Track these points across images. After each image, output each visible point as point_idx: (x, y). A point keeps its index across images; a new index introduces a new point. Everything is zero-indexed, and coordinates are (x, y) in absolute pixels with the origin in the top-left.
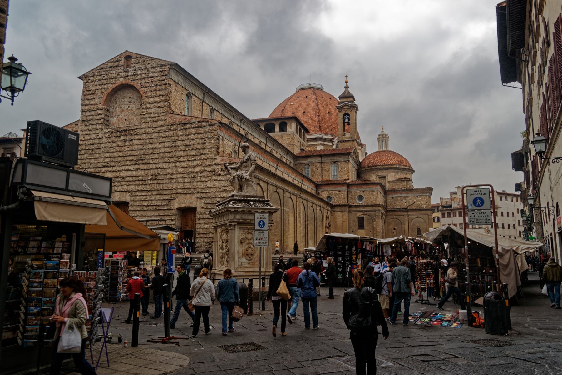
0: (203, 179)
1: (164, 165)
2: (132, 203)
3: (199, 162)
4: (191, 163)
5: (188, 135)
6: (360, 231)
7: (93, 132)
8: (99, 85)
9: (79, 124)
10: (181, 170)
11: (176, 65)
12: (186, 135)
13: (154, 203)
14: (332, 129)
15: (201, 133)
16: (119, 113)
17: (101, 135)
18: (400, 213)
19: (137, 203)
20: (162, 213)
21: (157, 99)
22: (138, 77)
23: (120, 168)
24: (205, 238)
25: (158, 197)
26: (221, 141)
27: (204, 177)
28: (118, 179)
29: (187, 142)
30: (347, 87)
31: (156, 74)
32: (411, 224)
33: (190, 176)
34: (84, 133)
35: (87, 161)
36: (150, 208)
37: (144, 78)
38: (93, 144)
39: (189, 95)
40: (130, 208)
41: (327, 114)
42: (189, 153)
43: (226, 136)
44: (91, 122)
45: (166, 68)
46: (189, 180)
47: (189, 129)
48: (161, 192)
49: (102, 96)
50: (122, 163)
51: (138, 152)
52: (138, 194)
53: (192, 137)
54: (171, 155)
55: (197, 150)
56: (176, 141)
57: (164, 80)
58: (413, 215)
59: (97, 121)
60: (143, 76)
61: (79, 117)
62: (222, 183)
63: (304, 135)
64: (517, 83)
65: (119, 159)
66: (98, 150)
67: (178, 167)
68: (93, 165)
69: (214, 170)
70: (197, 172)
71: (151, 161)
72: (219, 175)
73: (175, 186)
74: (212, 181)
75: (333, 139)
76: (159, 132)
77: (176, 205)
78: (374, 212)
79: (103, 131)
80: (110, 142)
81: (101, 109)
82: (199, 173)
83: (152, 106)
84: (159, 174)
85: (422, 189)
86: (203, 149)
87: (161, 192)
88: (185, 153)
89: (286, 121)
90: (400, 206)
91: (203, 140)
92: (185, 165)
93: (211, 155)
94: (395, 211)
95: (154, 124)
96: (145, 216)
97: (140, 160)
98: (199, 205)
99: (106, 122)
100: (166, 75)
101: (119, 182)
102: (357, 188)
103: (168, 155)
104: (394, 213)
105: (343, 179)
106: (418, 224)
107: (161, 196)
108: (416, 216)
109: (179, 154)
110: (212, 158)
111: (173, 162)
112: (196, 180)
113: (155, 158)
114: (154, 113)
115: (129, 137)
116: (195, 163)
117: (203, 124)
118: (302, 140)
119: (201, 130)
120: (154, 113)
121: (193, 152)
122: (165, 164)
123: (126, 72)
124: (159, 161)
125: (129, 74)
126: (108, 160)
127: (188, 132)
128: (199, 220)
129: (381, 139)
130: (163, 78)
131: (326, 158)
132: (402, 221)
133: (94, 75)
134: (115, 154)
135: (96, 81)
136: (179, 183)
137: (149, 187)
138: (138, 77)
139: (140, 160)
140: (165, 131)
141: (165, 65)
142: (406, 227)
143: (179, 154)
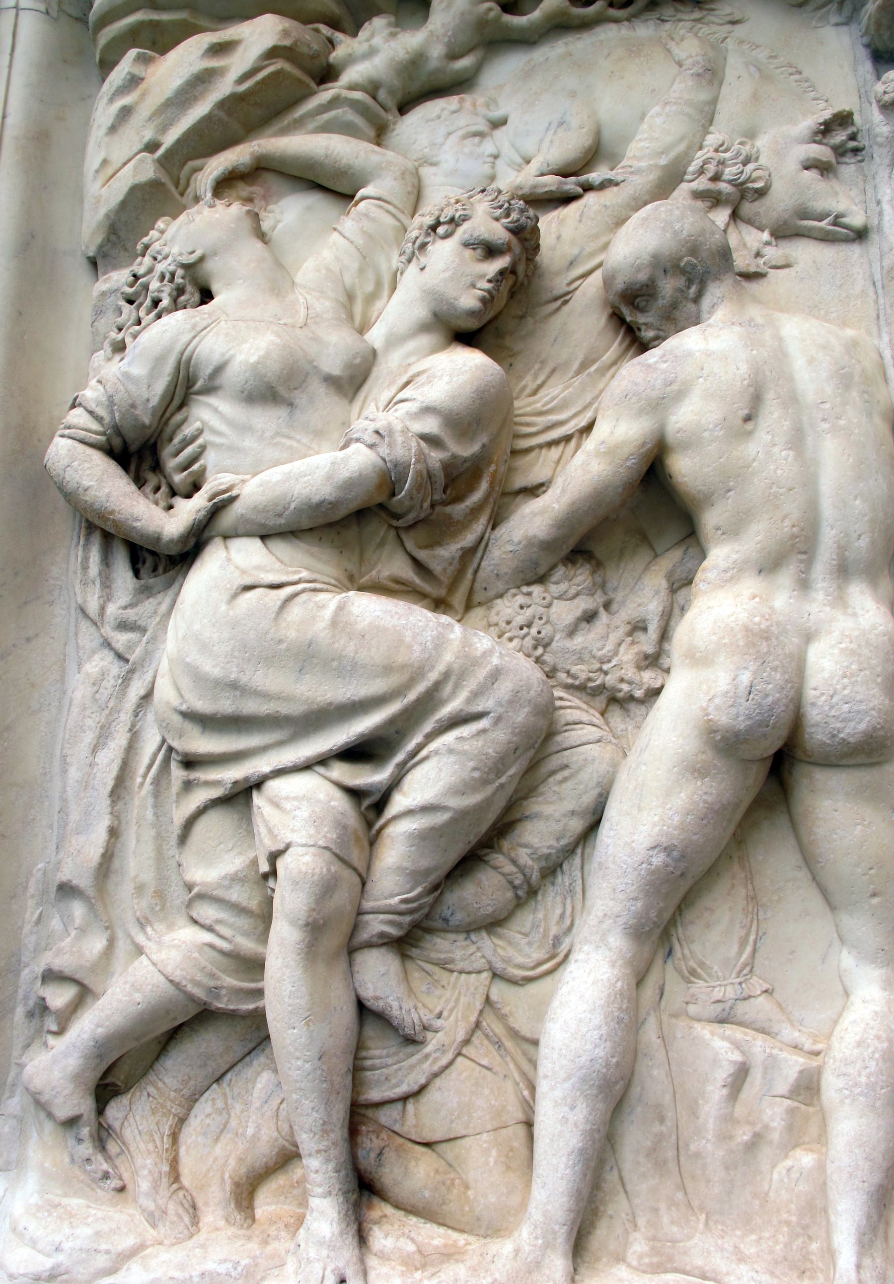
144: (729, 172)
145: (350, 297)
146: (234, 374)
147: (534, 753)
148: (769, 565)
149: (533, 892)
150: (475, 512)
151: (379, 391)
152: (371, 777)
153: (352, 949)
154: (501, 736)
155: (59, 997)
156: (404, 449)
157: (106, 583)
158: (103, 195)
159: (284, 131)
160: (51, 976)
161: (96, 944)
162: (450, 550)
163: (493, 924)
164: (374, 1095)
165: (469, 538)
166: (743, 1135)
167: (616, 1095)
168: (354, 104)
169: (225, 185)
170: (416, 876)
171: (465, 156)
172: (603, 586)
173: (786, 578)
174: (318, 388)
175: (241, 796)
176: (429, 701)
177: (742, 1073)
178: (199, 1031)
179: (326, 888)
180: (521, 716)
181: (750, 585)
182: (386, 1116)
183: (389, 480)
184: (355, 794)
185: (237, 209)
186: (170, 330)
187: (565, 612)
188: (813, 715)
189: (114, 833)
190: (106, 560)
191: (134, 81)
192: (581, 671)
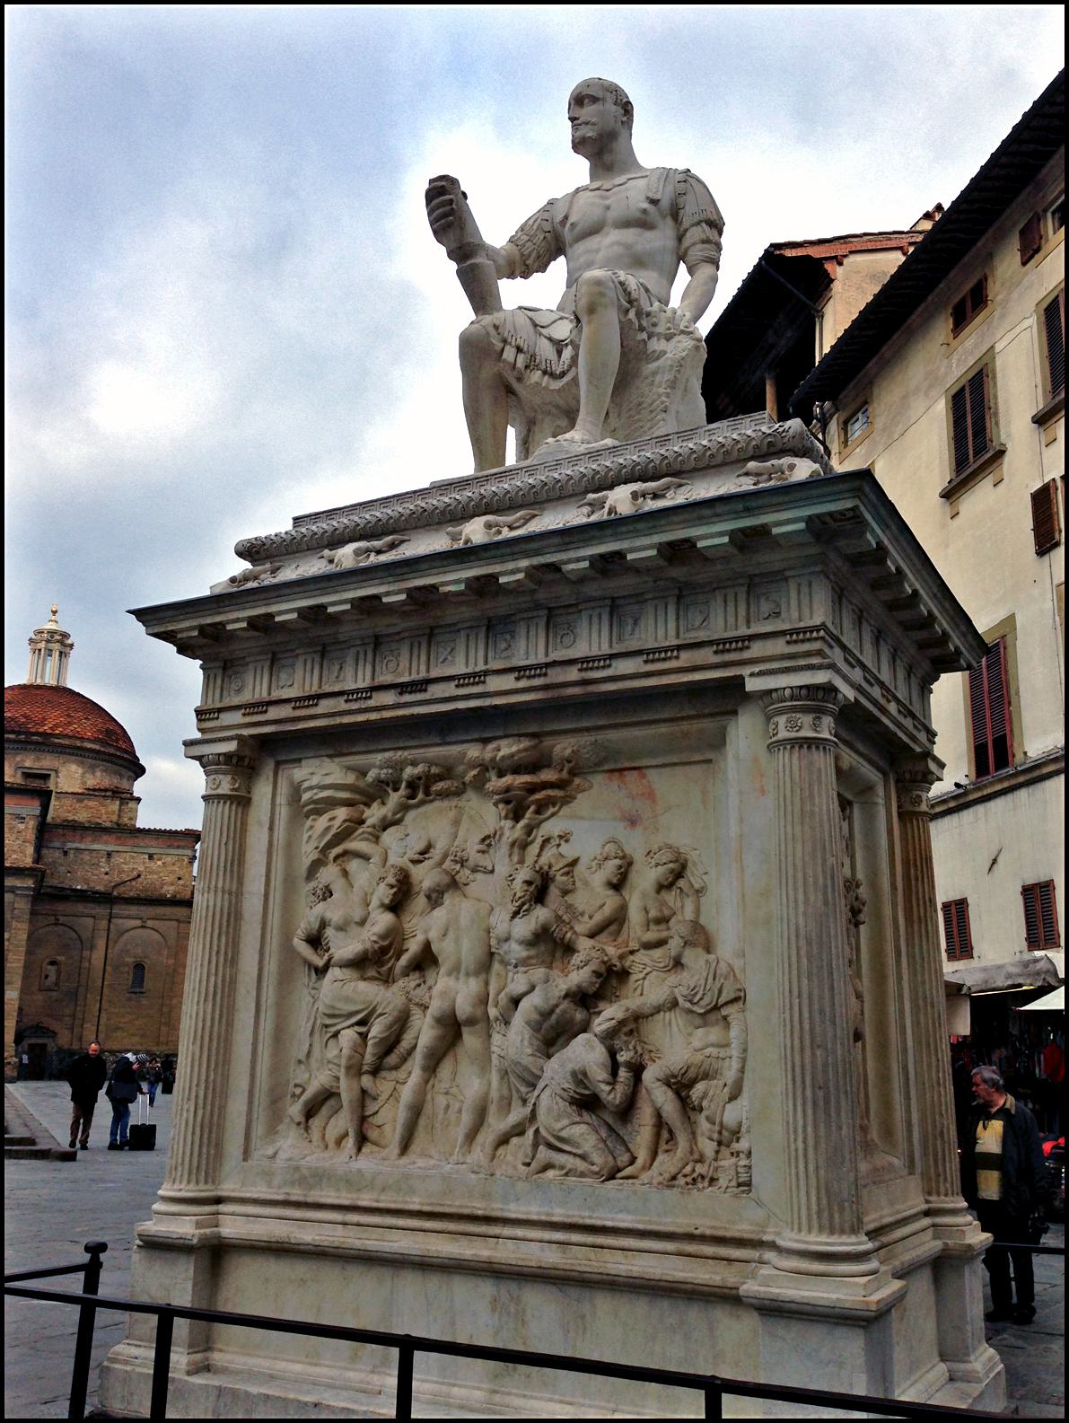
18: (80, 908)
32: (115, 951)
58: (128, 917)
85: (170, 832)
90: (86, 881)
104: (61, 907)
108: (138, 923)
129: (42, 645)
132: (85, 935)
142: (97, 956)
144: (459, 854)
145: (366, 895)
146: (333, 923)
148: (449, 974)
149: (406, 1060)
150: (390, 958)
151: (368, 925)
152: (363, 1029)
153: (360, 1074)
154: (391, 1018)
155: (298, 1091)
156: (368, 945)
157: (309, 976)
158: (306, 861)
159: (351, 841)
160: (296, 1086)
161: (307, 1075)
162: (385, 968)
163: (396, 1068)
164: (367, 1114)
165: (390, 965)
166: (446, 1123)
167: (416, 1111)
168: (369, 833)
169: (336, 859)
170: (374, 1055)
171: (398, 846)
172: (424, 976)
173: (452, 977)
174: (353, 925)
175: (336, 1035)
176: (374, 1010)
177: (448, 1107)
179: (350, 1058)
180: (395, 1013)
181: (446, 979)
182: (370, 1119)
183: (366, 952)
184: (359, 1033)
185: (338, 868)
186: (320, 909)
187: (413, 984)
188: (457, 1013)
189: (311, 1045)
190: (309, 970)
191: (312, 827)
192: (417, 1000)
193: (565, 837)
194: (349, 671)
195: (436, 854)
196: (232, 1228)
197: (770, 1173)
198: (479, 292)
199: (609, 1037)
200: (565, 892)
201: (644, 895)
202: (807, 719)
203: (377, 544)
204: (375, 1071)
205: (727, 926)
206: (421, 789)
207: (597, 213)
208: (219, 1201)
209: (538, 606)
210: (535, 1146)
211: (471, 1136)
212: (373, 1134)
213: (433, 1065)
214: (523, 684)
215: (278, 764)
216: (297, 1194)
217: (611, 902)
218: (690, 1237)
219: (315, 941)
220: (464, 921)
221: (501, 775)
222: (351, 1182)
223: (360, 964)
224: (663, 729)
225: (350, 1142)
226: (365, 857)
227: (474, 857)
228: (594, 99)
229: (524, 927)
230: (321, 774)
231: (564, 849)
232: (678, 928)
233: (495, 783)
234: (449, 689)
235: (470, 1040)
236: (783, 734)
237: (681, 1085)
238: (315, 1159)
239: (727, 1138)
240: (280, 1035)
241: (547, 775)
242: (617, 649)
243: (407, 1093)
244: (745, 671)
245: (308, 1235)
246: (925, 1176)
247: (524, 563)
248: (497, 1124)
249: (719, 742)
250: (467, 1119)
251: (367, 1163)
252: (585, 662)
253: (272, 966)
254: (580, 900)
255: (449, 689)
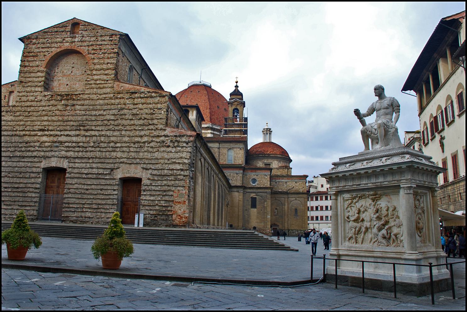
0: (151, 150)
1: (108, 133)
2: (70, 170)
3: (147, 133)
4: (137, 133)
5: (137, 104)
6: (253, 209)
7: (32, 94)
8: (42, 48)
9: (16, 85)
10: (126, 139)
11: (127, 35)
12: (134, 104)
13: (95, 171)
14: (220, 121)
15: (151, 104)
16: (60, 78)
17: (39, 98)
18: (282, 196)
19: (76, 171)
20: (103, 182)
21: (105, 66)
22: (85, 44)
23: (59, 133)
24: (151, 210)
25: (99, 165)
26: (169, 113)
27: (152, 147)
28: (55, 144)
29: (135, 111)
30: (237, 87)
31: (106, 43)
33: (136, 145)
34: (21, 94)
35: (22, 123)
36: (90, 176)
37: (92, 45)
38: (31, 106)
39: (131, 68)
40: (67, 175)
41: (217, 108)
42: (136, 122)
43: (174, 111)
44: (29, 84)
45: (116, 38)
46: (135, 150)
47: (138, 98)
48: (103, 160)
49: (44, 59)
50: (61, 128)
51: (80, 118)
52: (77, 160)
53: (140, 106)
54: (116, 123)
55: (146, 120)
56: (122, 109)
57: (113, 49)
58: (292, 198)
59: (36, 84)
60: (91, 43)
61: (16, 78)
62: (171, 155)
63: (201, 123)
64: (412, 91)
65: (58, 123)
66: (35, 113)
67: (124, 136)
68: (28, 128)
69: (163, 142)
70: (144, 143)
71: (93, 128)
72: (169, 146)
73: (119, 155)
74: (161, 152)
75: (221, 130)
76: (105, 98)
77: (119, 174)
78: (266, 194)
79: (43, 94)
80: (49, 106)
81: (42, 72)
82: (146, 144)
83: (99, 72)
84: (102, 142)
86: (152, 119)
87: (103, 160)
88: (132, 122)
89: (189, 109)
90: (282, 189)
91: (152, 111)
92: (131, 134)
93: (160, 126)
94: (277, 193)
95: (99, 91)
96: (84, 184)
97: (81, 126)
98: (145, 176)
99: (47, 86)
100: (115, 44)
101: (57, 147)
102: (252, 172)
103: (112, 122)
105: (238, 163)
106: (296, 206)
107: (103, 164)
109: (124, 122)
110: (161, 129)
111: (118, 130)
112: (143, 151)
113: (98, 125)
114: (100, 79)
115: (71, 102)
116: (142, 133)
117: (153, 94)
118: (199, 127)
119: (150, 100)
120: (100, 79)
121: (141, 122)
122: (109, 131)
123: (72, 38)
124: (103, 128)
125: (76, 40)
126: (45, 123)
127: (136, 101)
128: (144, 191)
129: (265, 132)
130: (113, 47)
131: (224, 144)
133: (37, 38)
134: (53, 118)
135: (39, 43)
136: (123, 152)
137: (89, 154)
138: (85, 44)
139: (81, 126)
140: (111, 98)
141: (116, 35)
142: (286, 207)
143: (124, 122)
147: (360, 228)
158: (346, 207)
163: (360, 234)
167: (363, 239)
171: (358, 205)
178: (351, 237)
193: (380, 204)
194: (349, 182)
195: (363, 206)
196: (341, 253)
197: (406, 245)
198: (363, 123)
199: (387, 230)
200: (381, 211)
201: (391, 212)
202: (408, 190)
203: (352, 164)
204: (357, 234)
205: (401, 216)
206: (361, 198)
207: (380, 107)
208: (339, 250)
209: (374, 175)
210: (378, 243)
211: (370, 242)
212: (358, 242)
213: (365, 233)
214: (373, 185)
215: (341, 194)
216: (349, 249)
217: (386, 213)
218: (397, 252)
219: (348, 218)
220: (368, 215)
221: (371, 196)
222: (355, 247)
223: (354, 221)
224: (392, 190)
225: (355, 243)
226: (354, 207)
227: (368, 207)
228: (378, 89)
229: (375, 216)
230: (347, 196)
231: (380, 206)
232: (395, 216)
233: (370, 197)
234: (363, 185)
235: (369, 230)
236: (406, 192)
237: (396, 235)
238: (351, 245)
239: (401, 241)
240: (344, 230)
241: (377, 196)
242: (385, 180)
243: (362, 237)
244: (401, 184)
245: (350, 254)
246: (436, 247)
247: (371, 170)
248: (373, 240)
249: (399, 192)
250: (370, 240)
251: (357, 245)
252: (381, 182)
253: (343, 221)
254: (383, 212)
255: (363, 185)
